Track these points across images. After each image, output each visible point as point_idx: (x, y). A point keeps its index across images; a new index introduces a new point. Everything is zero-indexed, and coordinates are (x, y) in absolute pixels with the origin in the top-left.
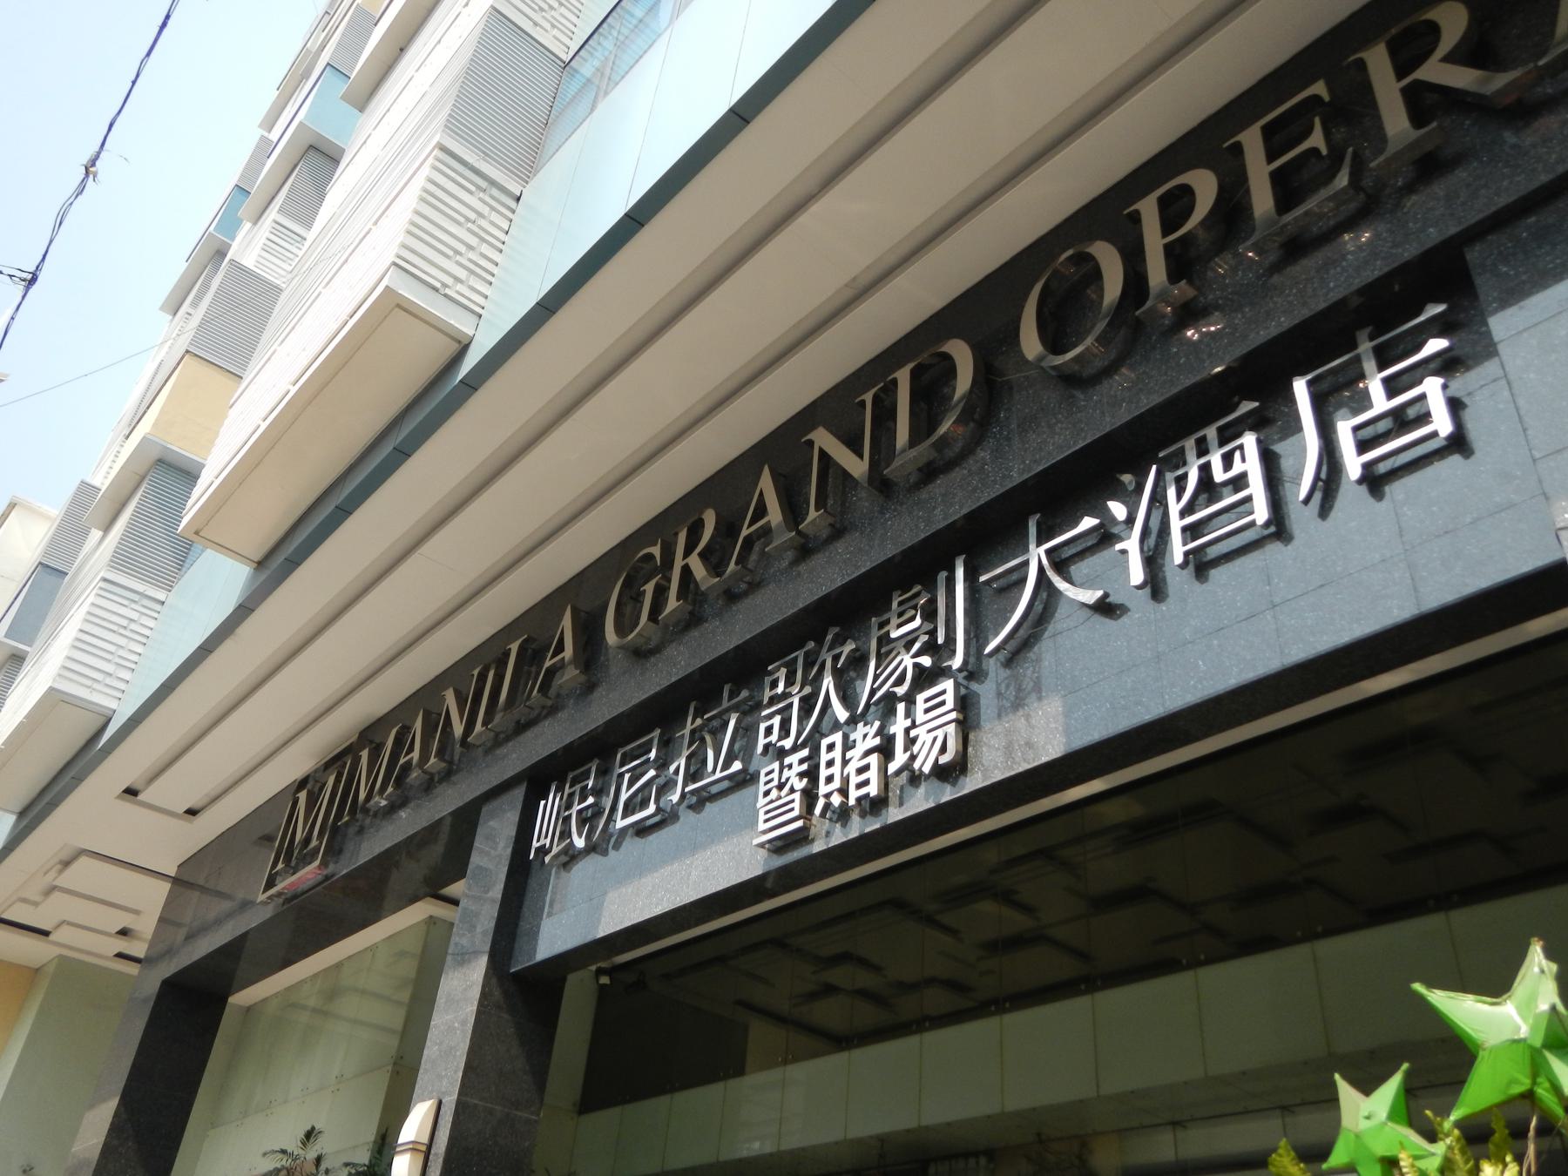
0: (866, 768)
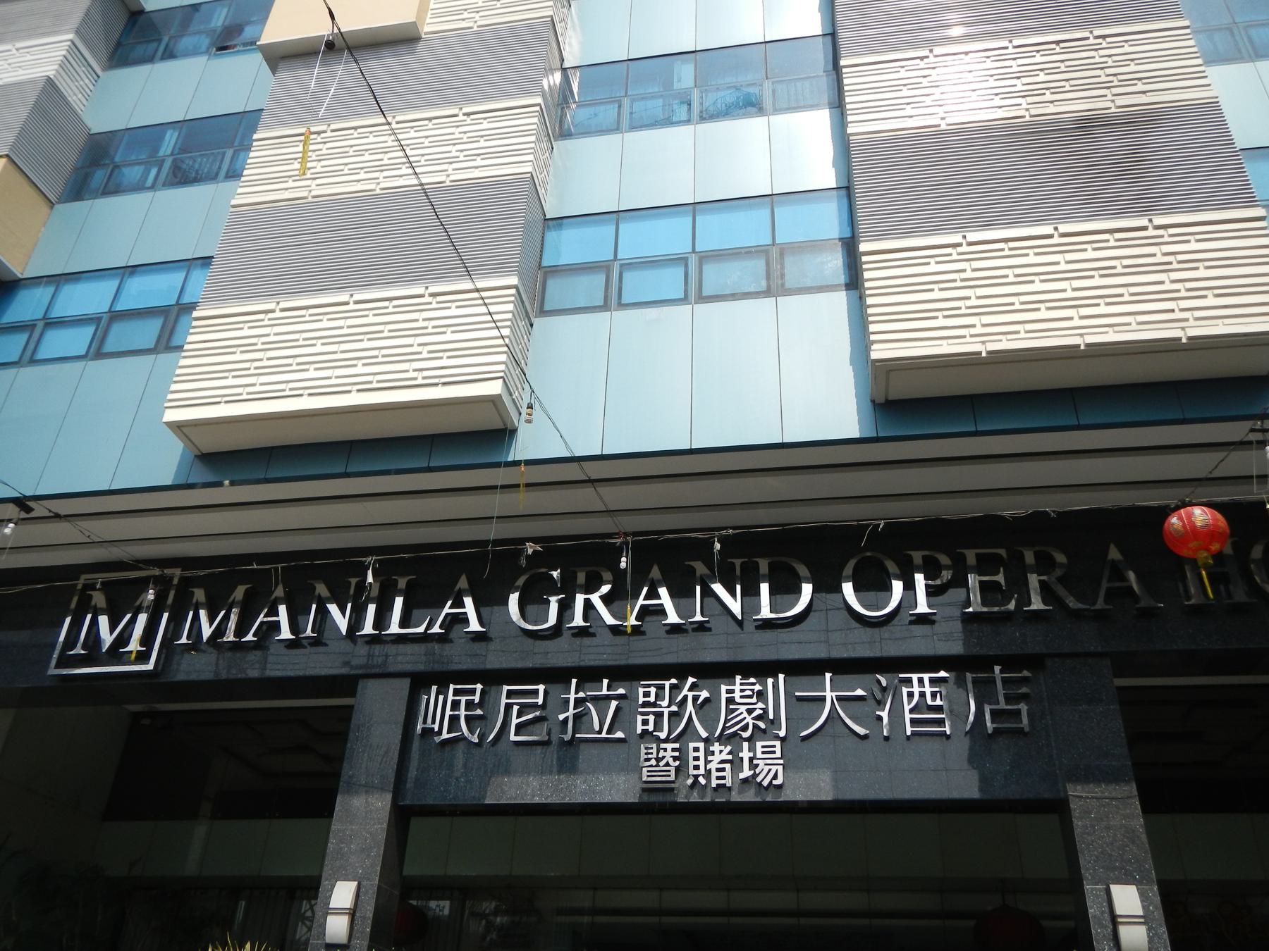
0: (723, 770)
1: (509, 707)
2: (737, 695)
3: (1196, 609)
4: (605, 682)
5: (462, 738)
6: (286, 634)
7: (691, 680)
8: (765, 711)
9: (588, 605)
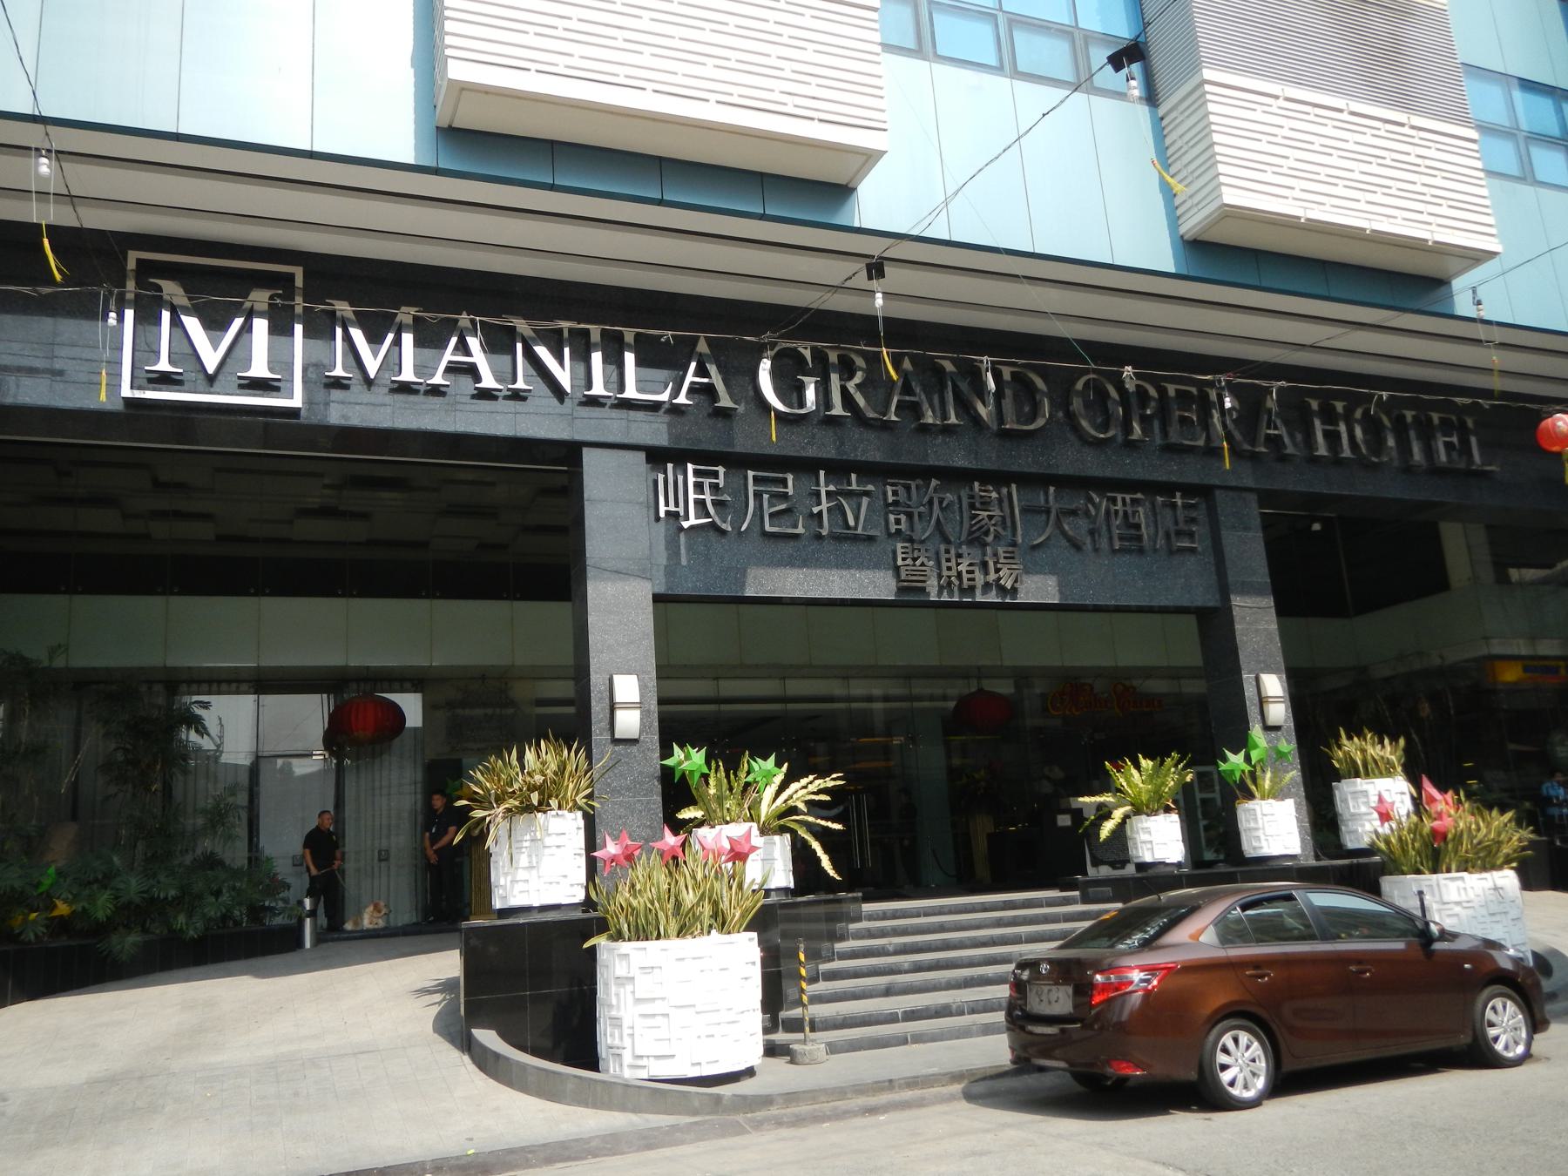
7: (934, 482)
9: (844, 391)
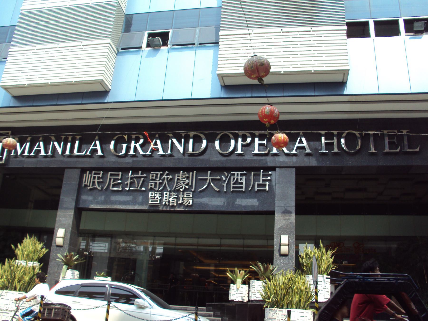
1: (110, 179)
2: (180, 178)
3: (336, 153)
4: (140, 172)
5: (96, 188)
6: (43, 153)
7: (167, 172)
8: (189, 183)
9: (135, 148)
